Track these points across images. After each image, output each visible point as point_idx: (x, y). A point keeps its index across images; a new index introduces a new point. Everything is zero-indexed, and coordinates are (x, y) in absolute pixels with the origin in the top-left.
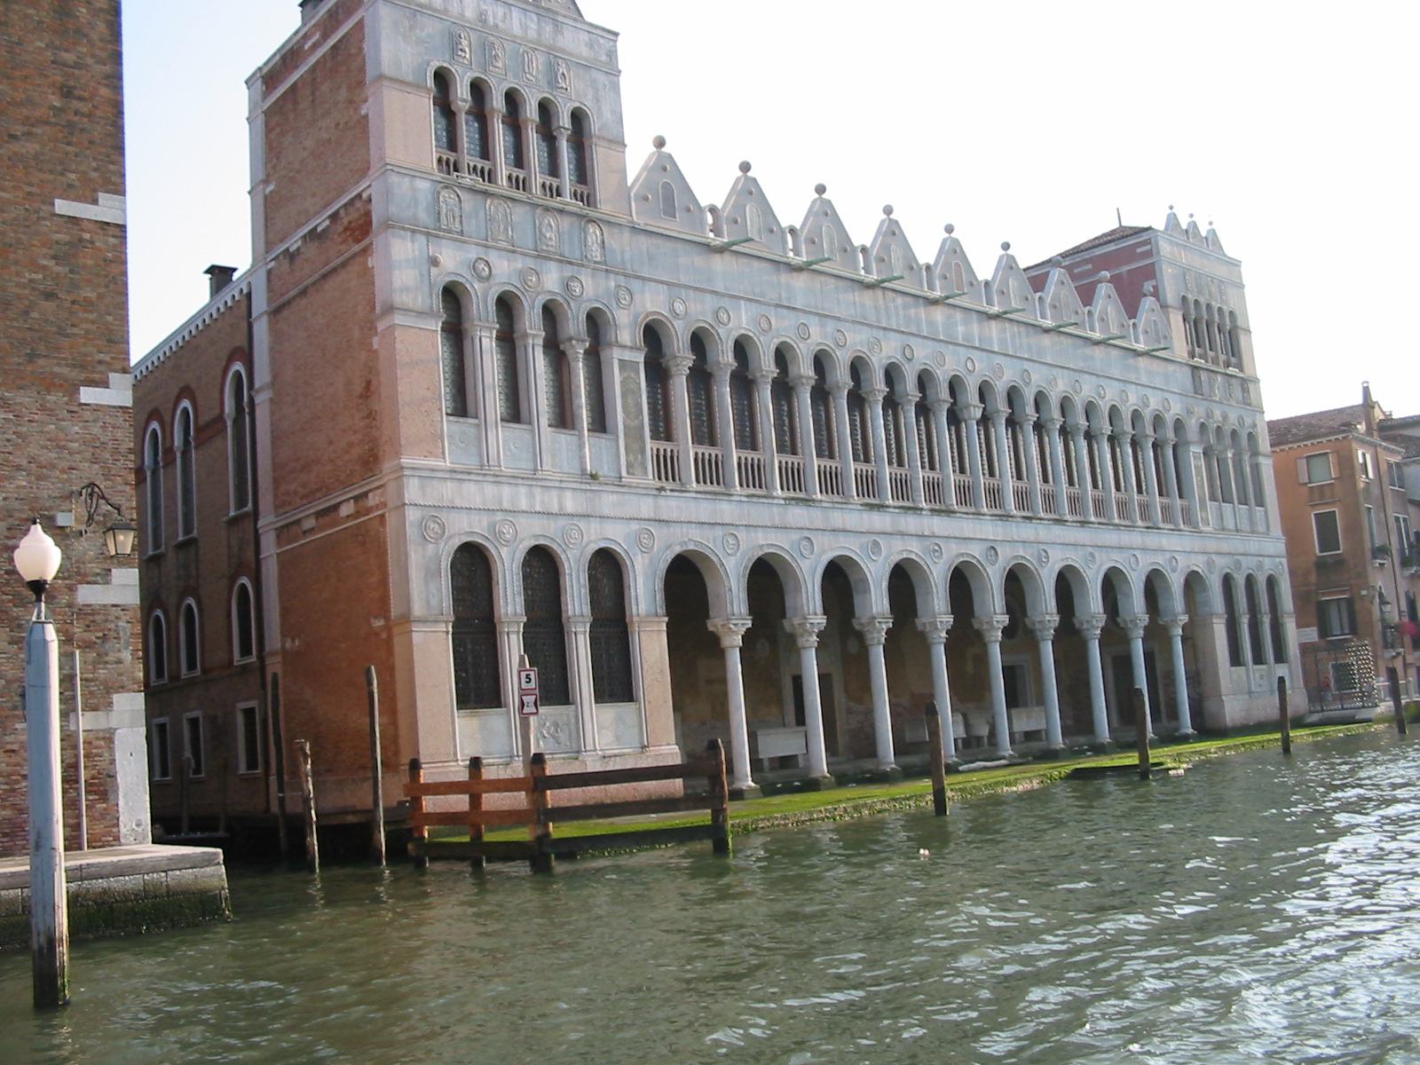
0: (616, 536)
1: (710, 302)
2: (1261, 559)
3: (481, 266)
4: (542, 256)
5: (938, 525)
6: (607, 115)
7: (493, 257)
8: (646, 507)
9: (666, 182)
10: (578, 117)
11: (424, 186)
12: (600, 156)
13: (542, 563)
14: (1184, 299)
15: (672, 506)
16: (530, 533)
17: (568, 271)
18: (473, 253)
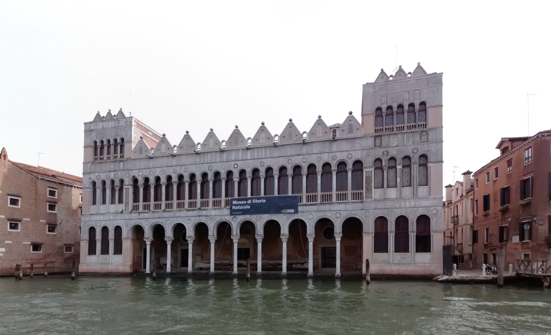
1: (148, 170)
2: (415, 209)
5: (213, 213)
6: (128, 136)
7: (101, 174)
9: (141, 147)
10: (122, 140)
11: (89, 165)
12: (126, 146)
13: (105, 230)
16: (103, 224)
17: (116, 173)
18: (97, 174)
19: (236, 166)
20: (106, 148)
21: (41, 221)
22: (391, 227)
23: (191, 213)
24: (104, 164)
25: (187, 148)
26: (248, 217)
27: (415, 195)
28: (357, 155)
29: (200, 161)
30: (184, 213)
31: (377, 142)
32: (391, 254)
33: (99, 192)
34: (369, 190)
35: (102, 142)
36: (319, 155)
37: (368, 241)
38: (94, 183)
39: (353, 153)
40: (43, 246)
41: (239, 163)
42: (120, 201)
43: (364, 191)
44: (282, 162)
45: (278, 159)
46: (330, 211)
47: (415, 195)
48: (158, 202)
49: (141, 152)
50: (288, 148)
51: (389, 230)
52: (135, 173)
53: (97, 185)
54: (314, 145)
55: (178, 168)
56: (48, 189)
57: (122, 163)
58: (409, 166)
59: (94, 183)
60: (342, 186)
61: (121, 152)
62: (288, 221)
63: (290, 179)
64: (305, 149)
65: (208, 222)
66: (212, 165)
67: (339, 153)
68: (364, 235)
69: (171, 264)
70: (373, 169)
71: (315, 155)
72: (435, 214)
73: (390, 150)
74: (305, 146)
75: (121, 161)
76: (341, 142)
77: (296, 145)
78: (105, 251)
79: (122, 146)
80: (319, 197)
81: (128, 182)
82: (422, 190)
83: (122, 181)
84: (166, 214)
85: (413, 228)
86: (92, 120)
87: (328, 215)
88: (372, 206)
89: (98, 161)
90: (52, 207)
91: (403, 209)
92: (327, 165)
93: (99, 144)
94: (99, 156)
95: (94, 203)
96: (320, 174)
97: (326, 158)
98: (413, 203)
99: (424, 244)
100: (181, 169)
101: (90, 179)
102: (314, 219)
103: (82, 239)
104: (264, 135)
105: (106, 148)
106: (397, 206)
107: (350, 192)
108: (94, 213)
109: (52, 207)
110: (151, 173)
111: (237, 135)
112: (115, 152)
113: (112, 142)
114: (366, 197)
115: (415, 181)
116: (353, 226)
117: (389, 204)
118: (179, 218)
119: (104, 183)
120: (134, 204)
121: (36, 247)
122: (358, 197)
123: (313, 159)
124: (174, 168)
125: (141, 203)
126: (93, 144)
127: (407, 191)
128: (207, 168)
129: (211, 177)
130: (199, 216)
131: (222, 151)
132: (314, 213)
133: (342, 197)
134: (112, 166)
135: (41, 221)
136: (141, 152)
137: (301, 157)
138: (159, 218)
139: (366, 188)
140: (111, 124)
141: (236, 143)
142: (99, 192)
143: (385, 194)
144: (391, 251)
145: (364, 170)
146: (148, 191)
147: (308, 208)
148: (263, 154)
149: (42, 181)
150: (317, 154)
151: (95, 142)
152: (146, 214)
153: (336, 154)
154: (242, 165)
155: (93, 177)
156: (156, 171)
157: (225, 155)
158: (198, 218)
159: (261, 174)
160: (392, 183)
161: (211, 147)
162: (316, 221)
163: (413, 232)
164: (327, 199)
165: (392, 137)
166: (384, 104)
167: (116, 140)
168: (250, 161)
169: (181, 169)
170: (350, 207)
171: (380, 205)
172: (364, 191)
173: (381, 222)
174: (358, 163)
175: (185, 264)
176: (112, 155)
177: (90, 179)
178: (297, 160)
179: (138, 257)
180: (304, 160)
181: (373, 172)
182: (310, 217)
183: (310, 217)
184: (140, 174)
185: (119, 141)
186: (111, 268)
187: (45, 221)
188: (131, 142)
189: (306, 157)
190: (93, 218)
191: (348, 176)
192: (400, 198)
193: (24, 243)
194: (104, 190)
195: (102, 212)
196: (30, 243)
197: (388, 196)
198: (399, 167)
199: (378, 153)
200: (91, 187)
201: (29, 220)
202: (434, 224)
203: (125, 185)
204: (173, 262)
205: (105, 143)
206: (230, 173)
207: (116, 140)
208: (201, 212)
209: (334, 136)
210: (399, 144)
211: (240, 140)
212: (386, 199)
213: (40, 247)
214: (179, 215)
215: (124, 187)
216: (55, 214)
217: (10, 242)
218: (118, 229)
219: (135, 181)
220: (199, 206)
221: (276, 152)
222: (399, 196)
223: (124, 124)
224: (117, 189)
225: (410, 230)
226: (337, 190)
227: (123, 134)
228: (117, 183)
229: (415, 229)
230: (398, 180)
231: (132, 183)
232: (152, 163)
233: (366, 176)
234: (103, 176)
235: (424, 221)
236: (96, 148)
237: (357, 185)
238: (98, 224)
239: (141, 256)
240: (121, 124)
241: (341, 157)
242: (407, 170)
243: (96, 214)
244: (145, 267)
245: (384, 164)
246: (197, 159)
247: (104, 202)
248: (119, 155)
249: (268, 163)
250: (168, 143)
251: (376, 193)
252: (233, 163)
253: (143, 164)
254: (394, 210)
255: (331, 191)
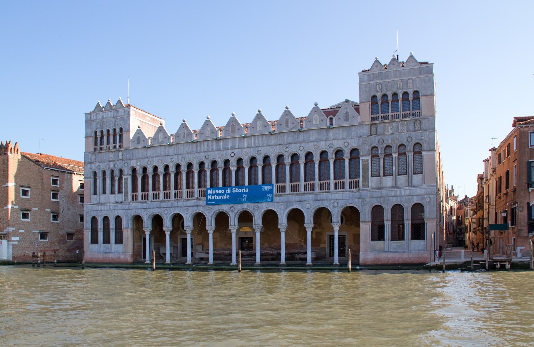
0: (120, 213)
1: (146, 160)
2: (409, 197)
3: (99, 167)
4: (110, 161)
6: (127, 126)
7: (101, 164)
8: (127, 207)
10: (121, 129)
11: (90, 155)
12: (125, 135)
14: (374, 97)
15: (133, 205)
16: (104, 214)
17: (115, 162)
18: (97, 164)
19: (233, 155)
20: (105, 138)
21: (46, 210)
22: (388, 216)
23: (189, 203)
24: (103, 154)
25: (184, 137)
26: (245, 207)
27: (410, 184)
28: (354, 143)
29: (197, 150)
30: (181, 203)
31: (372, 129)
32: (387, 242)
33: (99, 181)
34: (365, 179)
35: (102, 132)
36: (315, 143)
37: (365, 229)
38: (95, 173)
39: (349, 141)
40: (49, 235)
41: (236, 151)
42: (120, 192)
43: (361, 179)
44: (279, 150)
45: (275, 147)
46: (327, 199)
47: (410, 184)
48: (156, 192)
49: (139, 142)
50: (285, 136)
51: (385, 218)
52: (133, 163)
53: (97, 175)
54: (311, 133)
55: (175, 157)
56: (52, 178)
57: (120, 153)
58: (405, 154)
59: (95, 173)
60: (339, 175)
61: (120, 142)
62: (285, 210)
63: (288, 168)
64: (302, 136)
65: (206, 212)
66: (209, 153)
67: (336, 141)
68: (361, 224)
69: (171, 254)
70: (369, 158)
71: (312, 143)
72: (430, 202)
73: (386, 137)
74: (302, 134)
75: (120, 151)
76: (337, 129)
77: (293, 133)
78: (107, 241)
79: (121, 136)
80: (317, 186)
81: (127, 171)
82: (417, 178)
83: (121, 171)
84: (164, 204)
85: (408, 217)
86: (92, 110)
87: (326, 204)
88: (369, 194)
89: (98, 151)
90: (55, 196)
91: (399, 198)
92: (323, 153)
93: (99, 134)
94: (99, 146)
95: (95, 193)
96: (318, 162)
97: (323, 146)
98: (408, 191)
99: (418, 232)
100: (178, 159)
101: (91, 169)
102: (312, 208)
103: (85, 228)
104: (261, 122)
105: (105, 138)
106: (393, 195)
107: (347, 180)
108: (95, 202)
109: (55, 196)
110: (149, 163)
111: (234, 123)
112: (115, 142)
113: (111, 132)
114: (363, 185)
115: (410, 170)
116: (351, 215)
117: (384, 192)
118: (176, 208)
119: (104, 173)
120: (133, 194)
121: (43, 235)
122: (355, 185)
123: (310, 148)
124: (171, 157)
125: (140, 193)
126: (93, 135)
127: (402, 179)
128: (204, 157)
129: (208, 167)
130: (197, 206)
131: (218, 140)
132: (312, 203)
133: (340, 186)
134: (112, 156)
135: (46, 210)
136: (139, 142)
137: (298, 145)
138: (157, 208)
139: (363, 176)
140: (110, 114)
141: (233, 131)
142: (99, 181)
143: (381, 182)
144: (387, 240)
145: (361, 158)
146: (146, 181)
147: (306, 197)
148: (260, 142)
149: (46, 171)
150: (314, 142)
151: (96, 132)
152: (145, 204)
153: (333, 142)
154: (239, 154)
155: (94, 167)
156: (153, 161)
157: (221, 143)
158: (195, 208)
159: (258, 163)
160: (388, 172)
161: (207, 135)
162: (314, 211)
163: (408, 220)
164: (325, 187)
165: (387, 125)
166: (379, 92)
167: (115, 130)
168: (248, 150)
169: (178, 159)
170: (347, 195)
171: (377, 193)
172: (361, 179)
173: (377, 210)
174: (354, 151)
175: (184, 254)
176: (112, 145)
177: (91, 169)
178: (294, 148)
179: (138, 246)
180: (301, 148)
181: (370, 160)
182: (308, 206)
183: (308, 206)
184: (139, 163)
185: (118, 131)
186: (113, 256)
187: (49, 210)
188: (128, 131)
189: (303, 145)
190: (95, 208)
191: (345, 165)
192: (395, 186)
193: (34, 231)
194: (104, 180)
195: (102, 202)
196: (38, 232)
197: (384, 185)
198: (395, 155)
199: (374, 141)
200: (92, 177)
201: (37, 209)
202: (428, 212)
203: (124, 175)
204: (172, 252)
205: (105, 133)
206: (227, 162)
207: (115, 130)
208: (198, 202)
209: (331, 123)
210: (396, 132)
211: (236, 128)
212: (382, 188)
213: (47, 235)
214: (176, 205)
215: (123, 177)
216: (58, 202)
217: (23, 231)
218: (118, 219)
219: (134, 170)
220: (196, 196)
221: (273, 140)
222: (394, 185)
223: (123, 114)
224: (117, 178)
225: (405, 218)
226: (335, 179)
227: (121, 124)
228: (116, 173)
229: (410, 217)
230: (394, 168)
231: (130, 172)
232: (149, 152)
233: (362, 164)
234: (103, 166)
235: (418, 208)
236: (96, 138)
237: (354, 174)
238: (100, 214)
239: (141, 246)
240: (119, 114)
241: (338, 144)
242: (402, 158)
243: (97, 204)
244: (145, 257)
245: (379, 152)
246: (194, 148)
247: (104, 192)
248: (118, 144)
249: (265, 151)
250: (165, 133)
251: (373, 182)
252: (230, 152)
253: (141, 153)
254: (390, 198)
255: (329, 179)
